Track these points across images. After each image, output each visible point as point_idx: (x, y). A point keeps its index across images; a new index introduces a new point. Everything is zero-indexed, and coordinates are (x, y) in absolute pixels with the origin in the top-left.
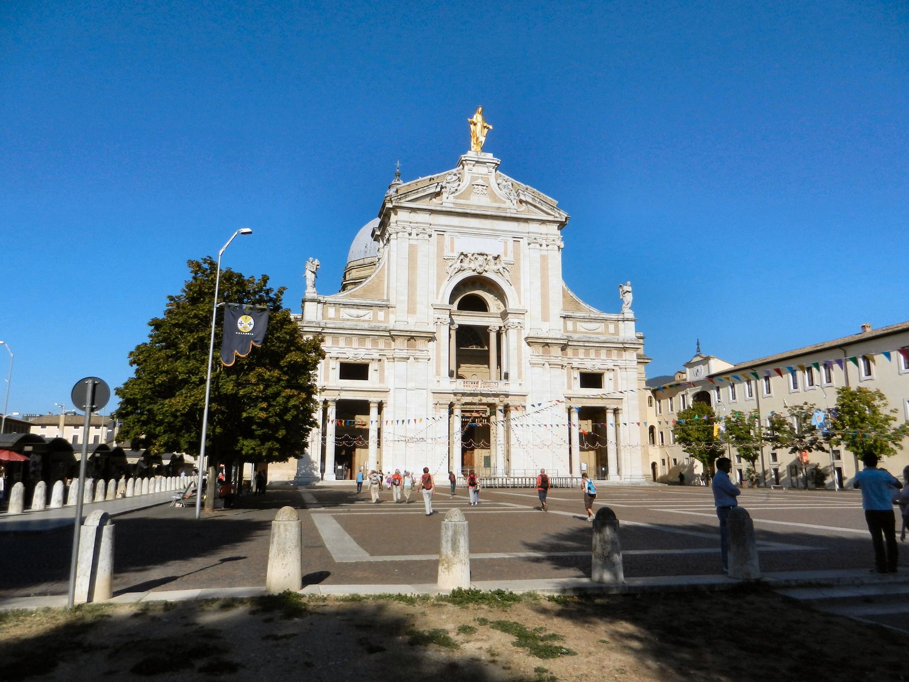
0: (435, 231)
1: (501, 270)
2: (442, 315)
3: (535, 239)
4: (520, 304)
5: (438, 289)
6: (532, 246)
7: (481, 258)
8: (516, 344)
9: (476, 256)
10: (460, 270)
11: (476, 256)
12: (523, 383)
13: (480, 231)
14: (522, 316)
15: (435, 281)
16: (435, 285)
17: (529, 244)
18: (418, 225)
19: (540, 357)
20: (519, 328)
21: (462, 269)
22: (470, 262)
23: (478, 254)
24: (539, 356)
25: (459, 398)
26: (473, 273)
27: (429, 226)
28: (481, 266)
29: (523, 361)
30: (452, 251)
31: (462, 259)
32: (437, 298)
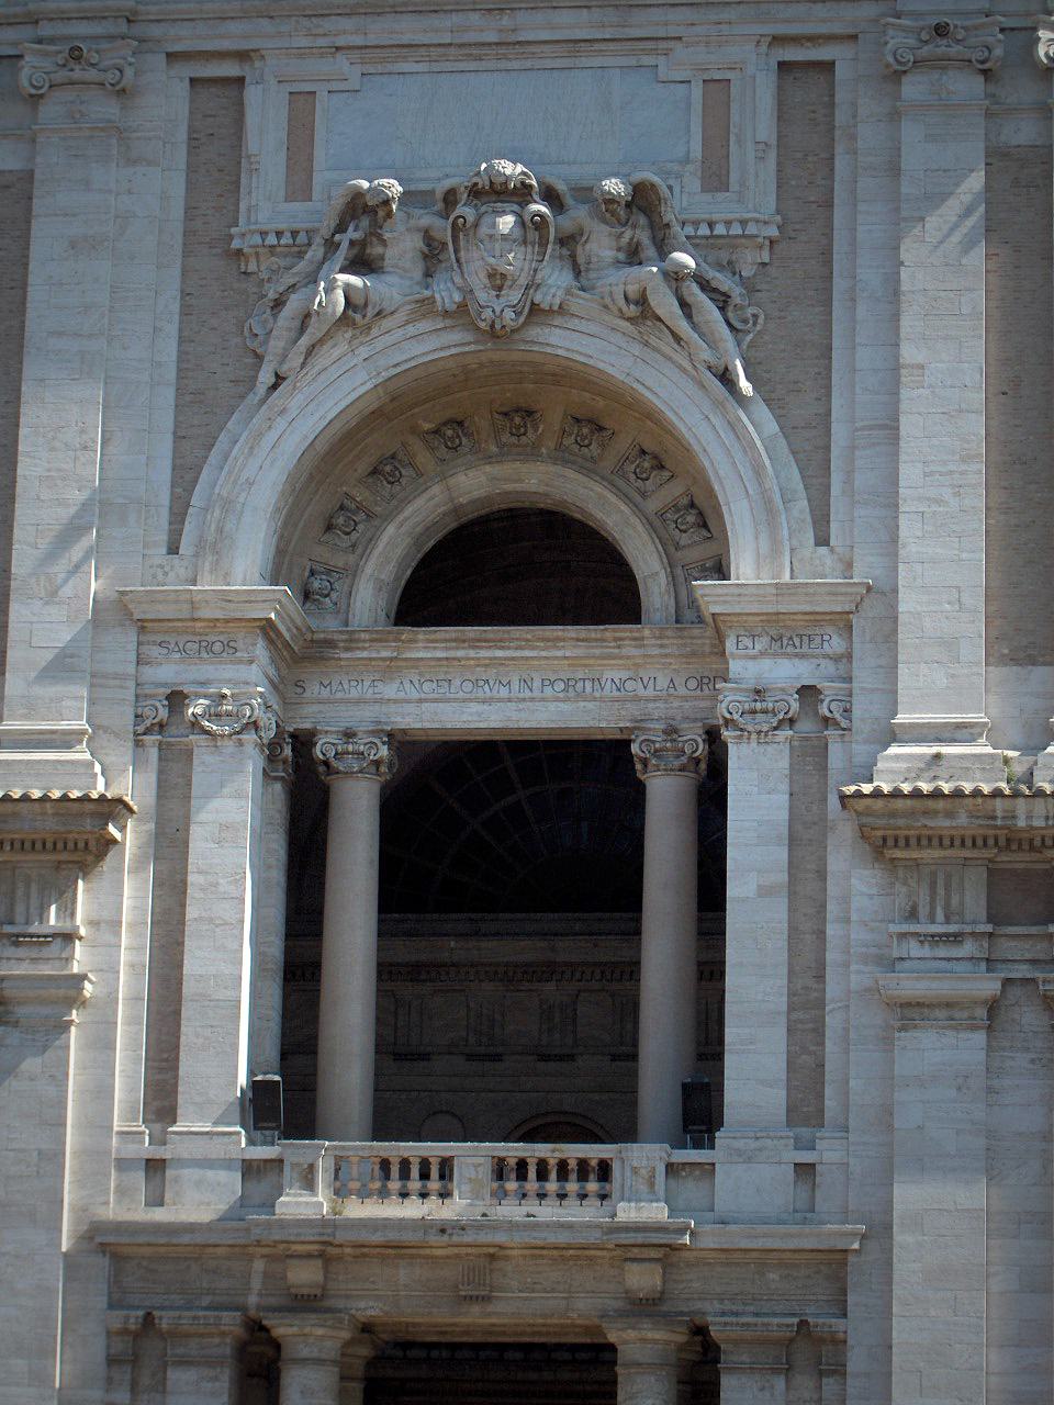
0: (170, 56)
1: (664, 303)
2: (207, 671)
3: (941, 31)
4: (822, 540)
5: (185, 476)
6: (913, 88)
7: (506, 223)
8: (782, 854)
9: (466, 211)
10: (344, 320)
11: (466, 211)
12: (828, 1152)
13: (506, 21)
14: (836, 644)
15: (167, 420)
16: (165, 446)
17: (896, 76)
18: (46, 30)
19: (968, 948)
20: (806, 726)
21: (358, 317)
22: (425, 257)
23: (475, 193)
24: (956, 938)
25: (304, 1275)
26: (456, 336)
27: (123, 28)
28: (498, 280)
29: (833, 989)
30: (299, 184)
31: (352, 243)
32: (173, 549)
